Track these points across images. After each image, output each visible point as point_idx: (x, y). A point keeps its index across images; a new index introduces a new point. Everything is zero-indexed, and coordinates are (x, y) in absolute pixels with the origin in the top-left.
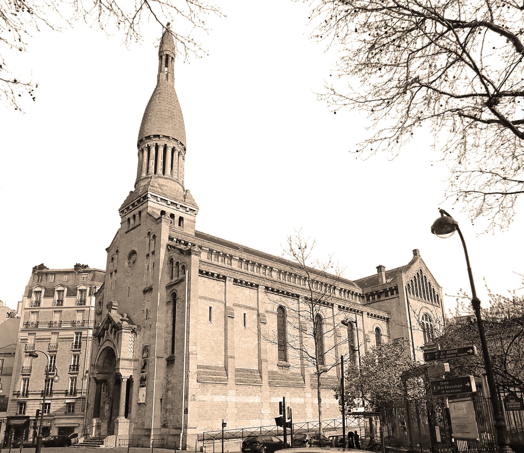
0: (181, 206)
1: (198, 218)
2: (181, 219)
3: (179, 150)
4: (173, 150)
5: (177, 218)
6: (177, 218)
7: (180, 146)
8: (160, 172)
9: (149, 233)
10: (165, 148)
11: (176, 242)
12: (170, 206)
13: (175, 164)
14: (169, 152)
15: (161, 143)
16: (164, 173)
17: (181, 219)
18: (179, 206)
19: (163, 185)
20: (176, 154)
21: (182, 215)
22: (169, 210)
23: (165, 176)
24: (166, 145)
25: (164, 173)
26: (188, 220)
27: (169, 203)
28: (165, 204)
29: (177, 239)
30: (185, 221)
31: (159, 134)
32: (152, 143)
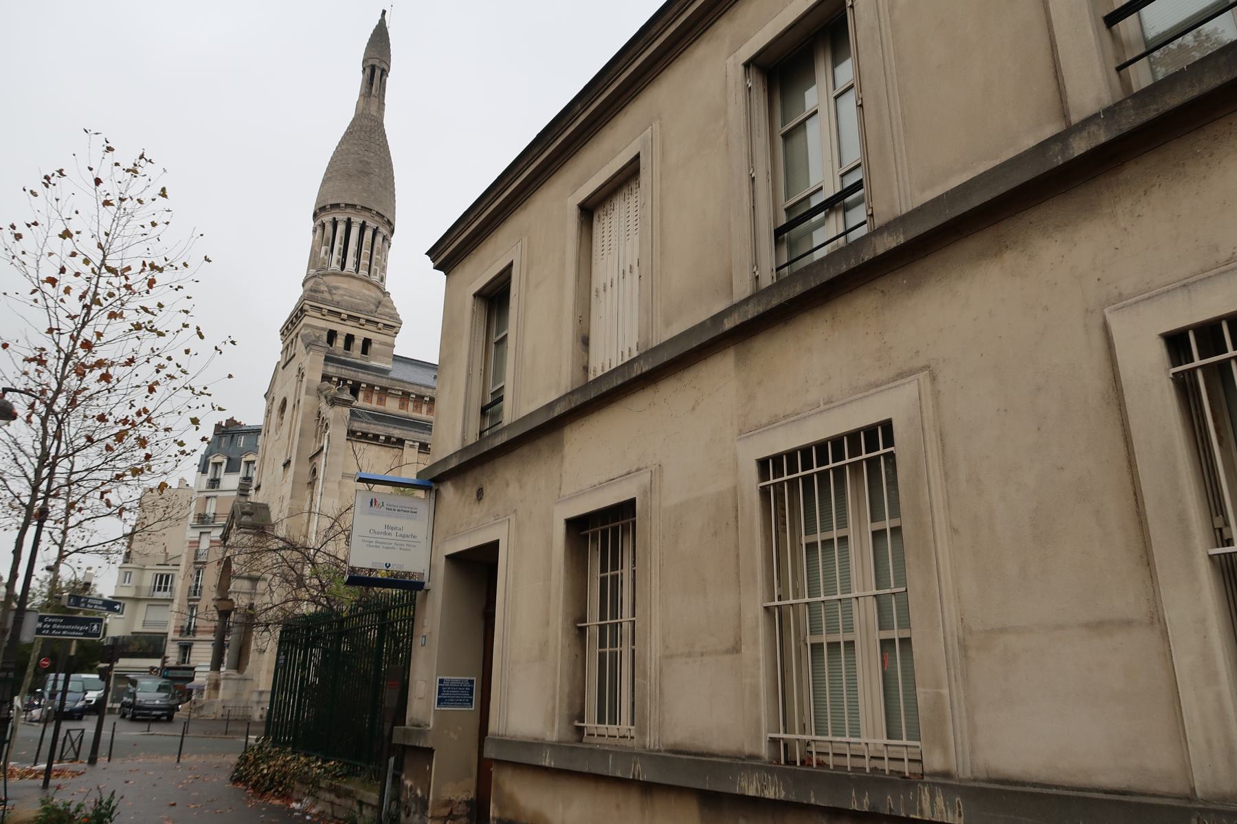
0: (367, 321)
1: (398, 341)
2: (367, 343)
3: (374, 226)
4: (363, 227)
5: (358, 343)
6: (358, 343)
12: (348, 323)
13: (365, 251)
14: (355, 232)
15: (341, 217)
16: (343, 267)
19: (337, 288)
20: (368, 234)
22: (343, 329)
24: (349, 219)
26: (381, 343)
29: (340, 379)
30: (374, 346)
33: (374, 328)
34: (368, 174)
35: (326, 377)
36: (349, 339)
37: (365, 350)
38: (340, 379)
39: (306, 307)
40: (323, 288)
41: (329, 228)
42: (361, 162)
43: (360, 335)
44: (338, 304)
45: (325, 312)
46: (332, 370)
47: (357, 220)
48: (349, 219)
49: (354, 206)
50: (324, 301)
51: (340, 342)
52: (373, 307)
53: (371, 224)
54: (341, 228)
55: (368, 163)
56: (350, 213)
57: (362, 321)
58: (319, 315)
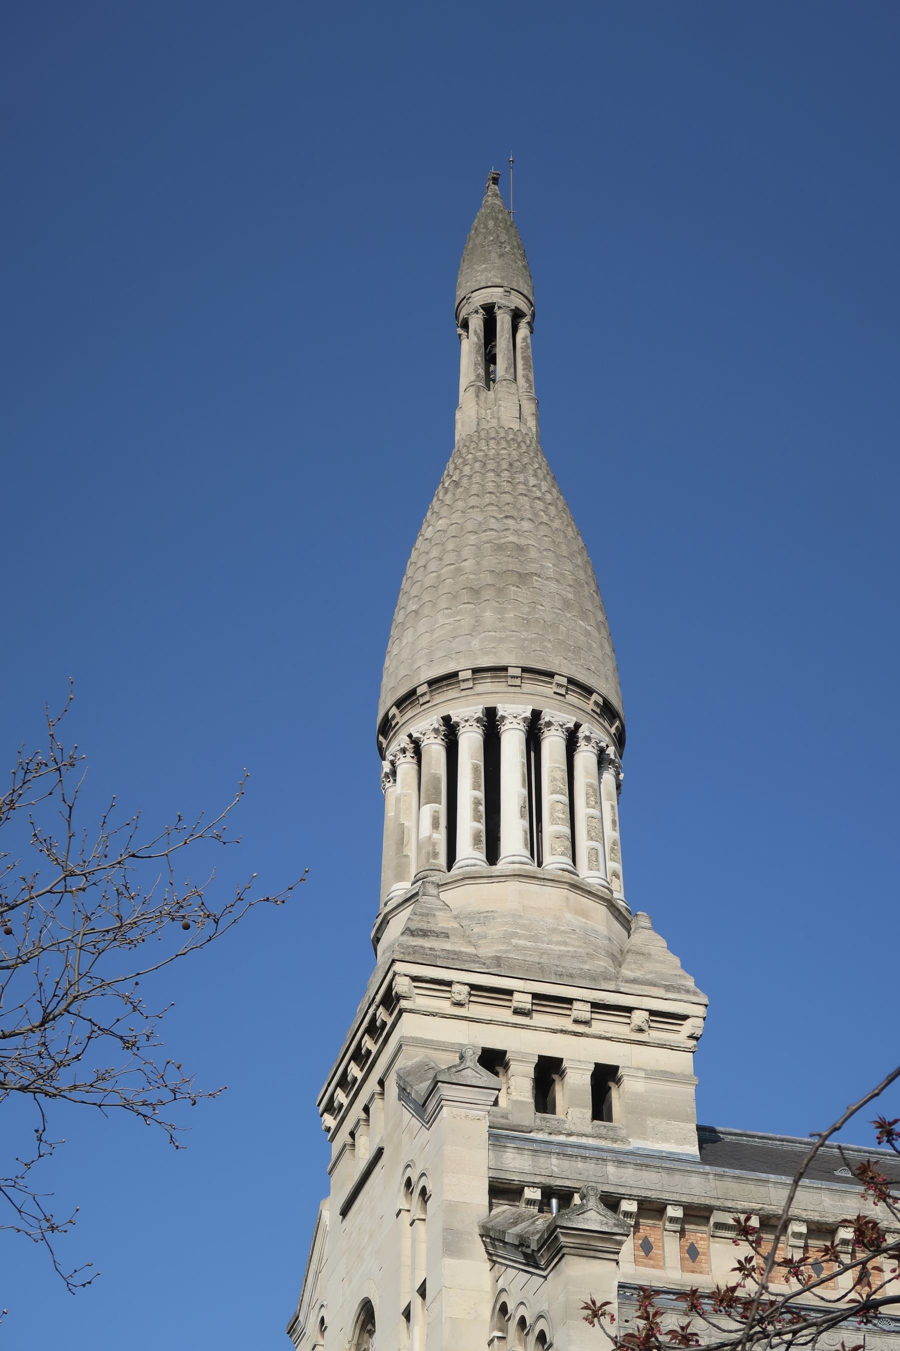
0: (597, 1006)
2: (604, 1078)
7: (572, 698)
8: (469, 851)
9: (408, 1183)
10: (491, 724)
11: (543, 1205)
12: (538, 1019)
13: (552, 798)
15: (466, 709)
16: (493, 855)
17: (604, 1078)
18: (582, 1010)
20: (553, 745)
21: (609, 1054)
23: (502, 866)
24: (491, 713)
25: (493, 855)
27: (523, 1000)
28: (506, 1015)
29: (548, 1192)
31: (450, 668)
32: (423, 723)
33: (624, 1031)
34: (523, 578)
35: (502, 1191)
36: (548, 1071)
37: (601, 1108)
38: (548, 1192)
39: (402, 985)
40: (443, 922)
41: (435, 751)
42: (500, 548)
43: (580, 1057)
44: (498, 965)
45: (460, 992)
46: (517, 1164)
47: (514, 711)
48: (491, 713)
49: (499, 670)
50: (454, 960)
51: (520, 1084)
52: (603, 964)
53: (558, 715)
54: (470, 742)
55: (520, 548)
56: (489, 694)
57: (582, 1010)
58: (445, 1006)
